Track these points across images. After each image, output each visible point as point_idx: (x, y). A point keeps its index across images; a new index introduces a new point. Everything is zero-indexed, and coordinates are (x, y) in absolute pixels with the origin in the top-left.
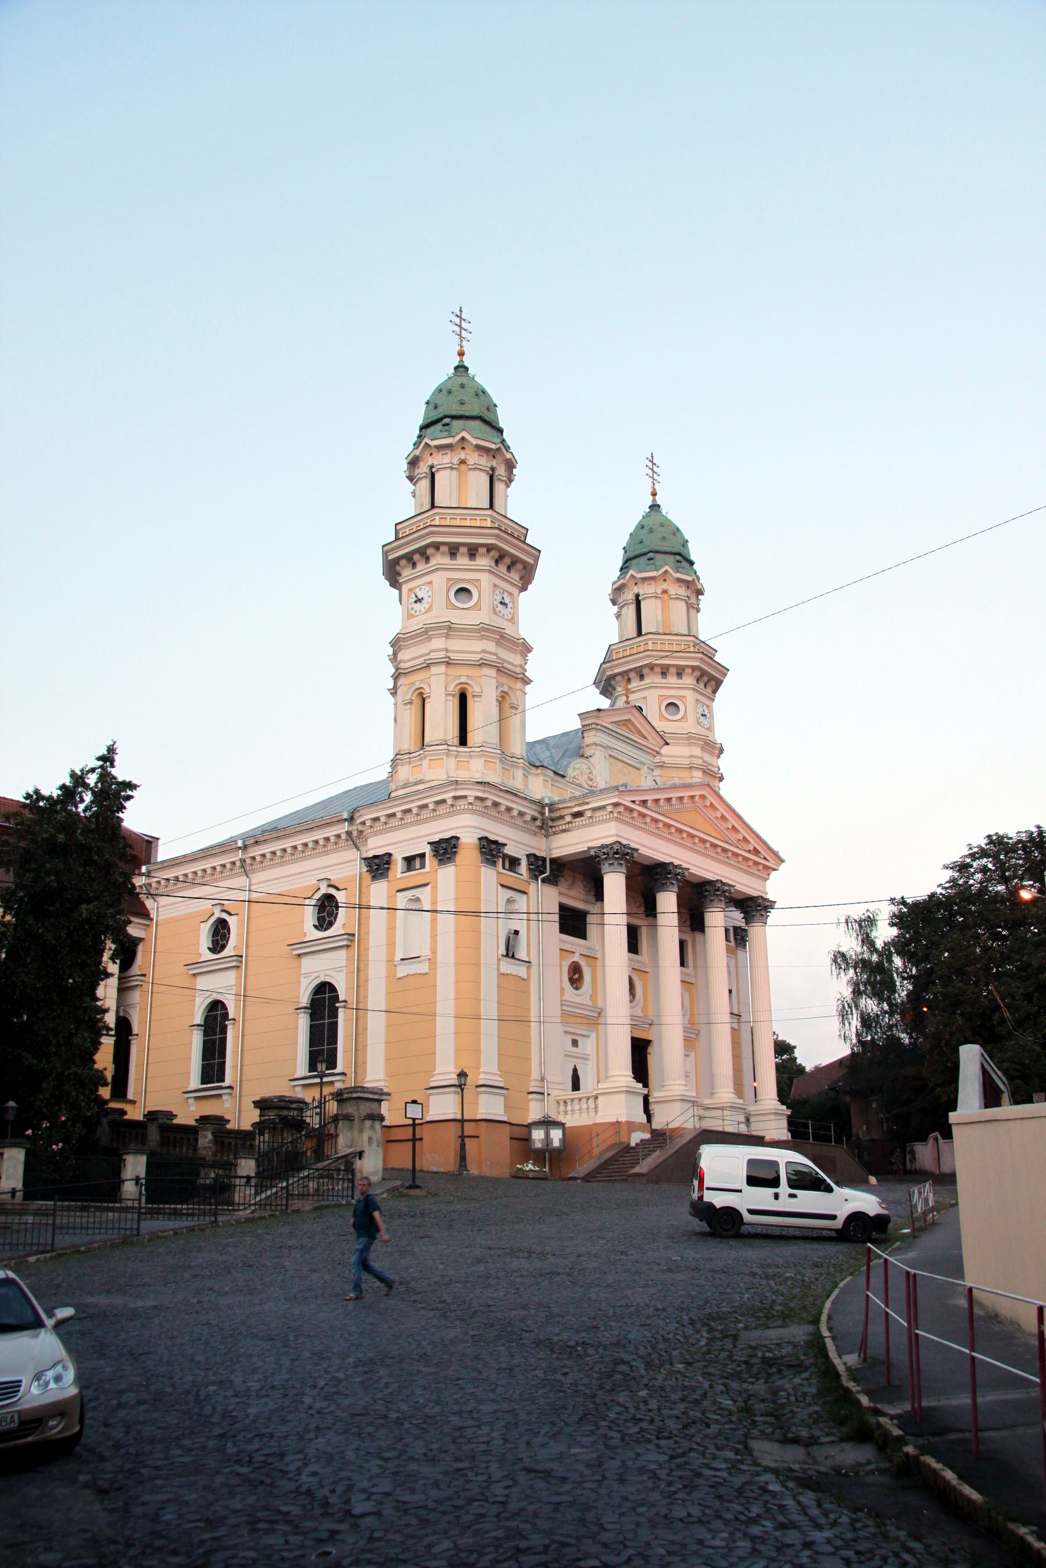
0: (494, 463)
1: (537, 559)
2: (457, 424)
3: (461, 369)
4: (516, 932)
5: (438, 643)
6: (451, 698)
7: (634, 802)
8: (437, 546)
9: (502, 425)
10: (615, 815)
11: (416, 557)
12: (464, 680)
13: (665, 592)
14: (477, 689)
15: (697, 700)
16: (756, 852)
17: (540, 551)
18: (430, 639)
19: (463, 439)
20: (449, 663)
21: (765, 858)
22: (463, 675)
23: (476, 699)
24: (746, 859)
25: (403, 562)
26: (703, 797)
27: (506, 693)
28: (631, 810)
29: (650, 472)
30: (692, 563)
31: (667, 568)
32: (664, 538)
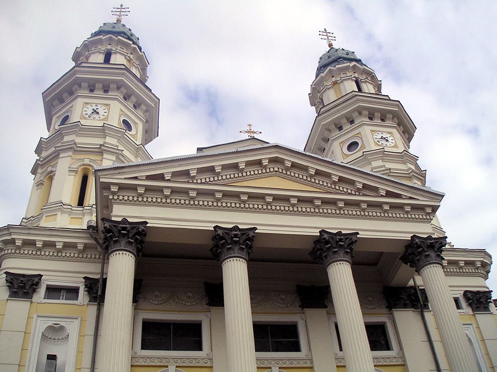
0: (109, 47)
4: (52, 358)
7: (136, 178)
10: (111, 197)
12: (50, 169)
13: (335, 83)
14: (54, 169)
15: (373, 131)
16: (389, 194)
21: (411, 198)
24: (371, 205)
26: (273, 161)
27: (89, 165)
28: (134, 188)
29: (326, 37)
30: (359, 61)
31: (329, 68)
32: (329, 57)
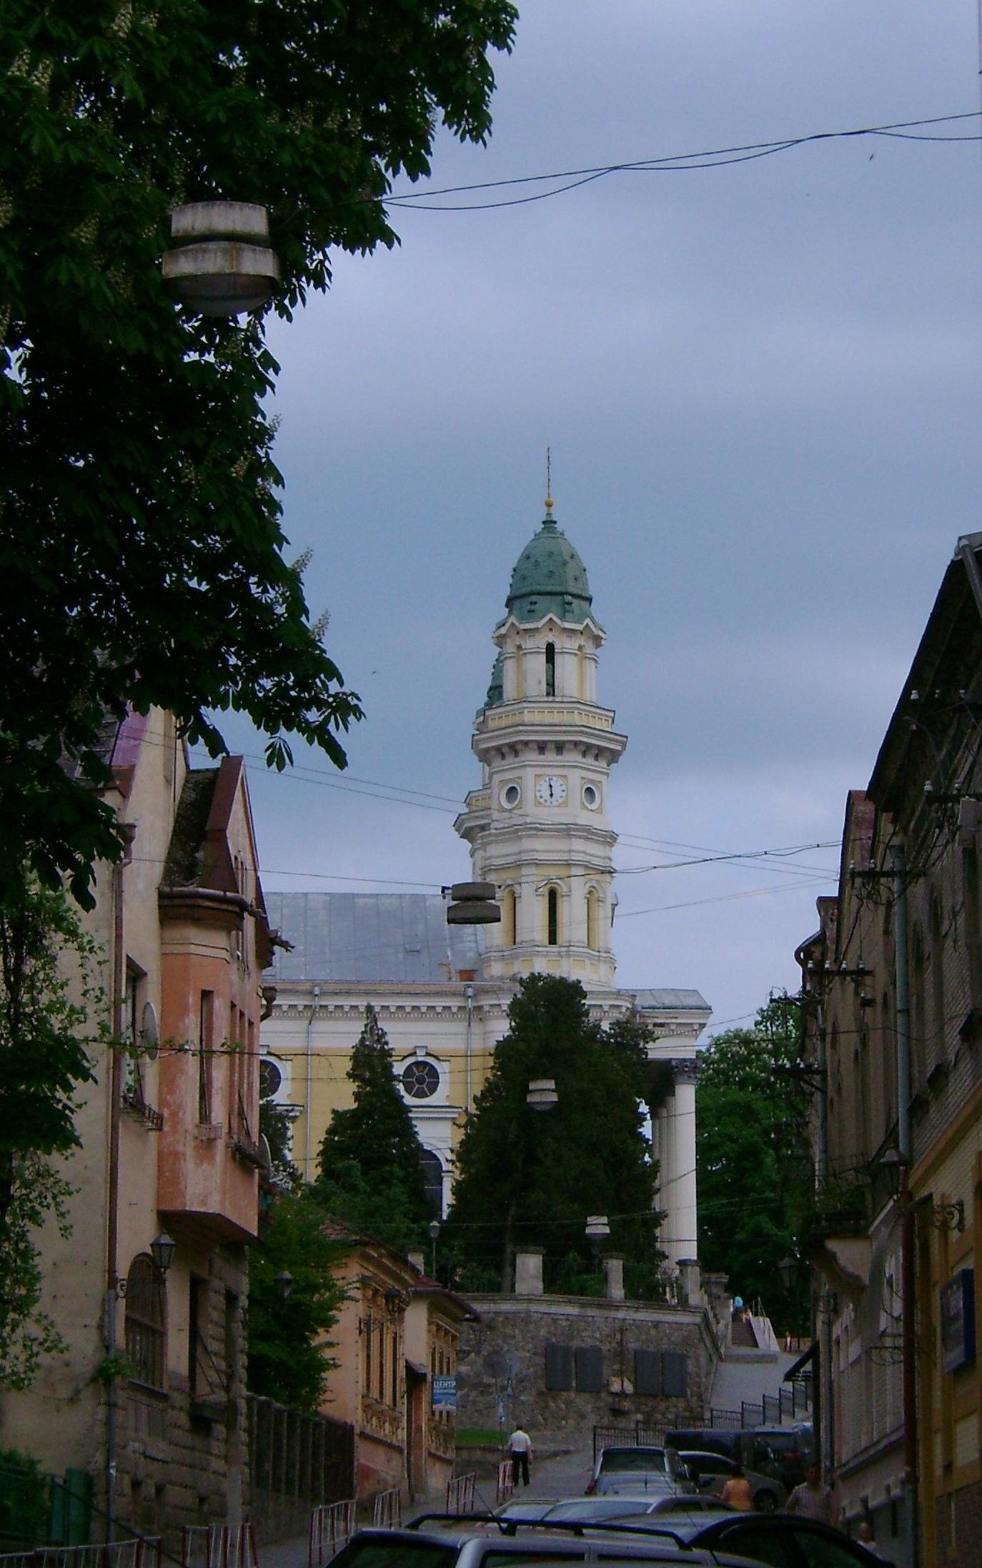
1: (624, 745)
2: (543, 602)
3: (549, 523)
5: (527, 844)
6: (540, 898)
8: (526, 743)
9: (592, 591)
11: (505, 750)
14: (565, 889)
17: (626, 737)
18: (520, 838)
19: (551, 619)
20: (537, 864)
22: (553, 872)
23: (565, 898)
25: (493, 753)
